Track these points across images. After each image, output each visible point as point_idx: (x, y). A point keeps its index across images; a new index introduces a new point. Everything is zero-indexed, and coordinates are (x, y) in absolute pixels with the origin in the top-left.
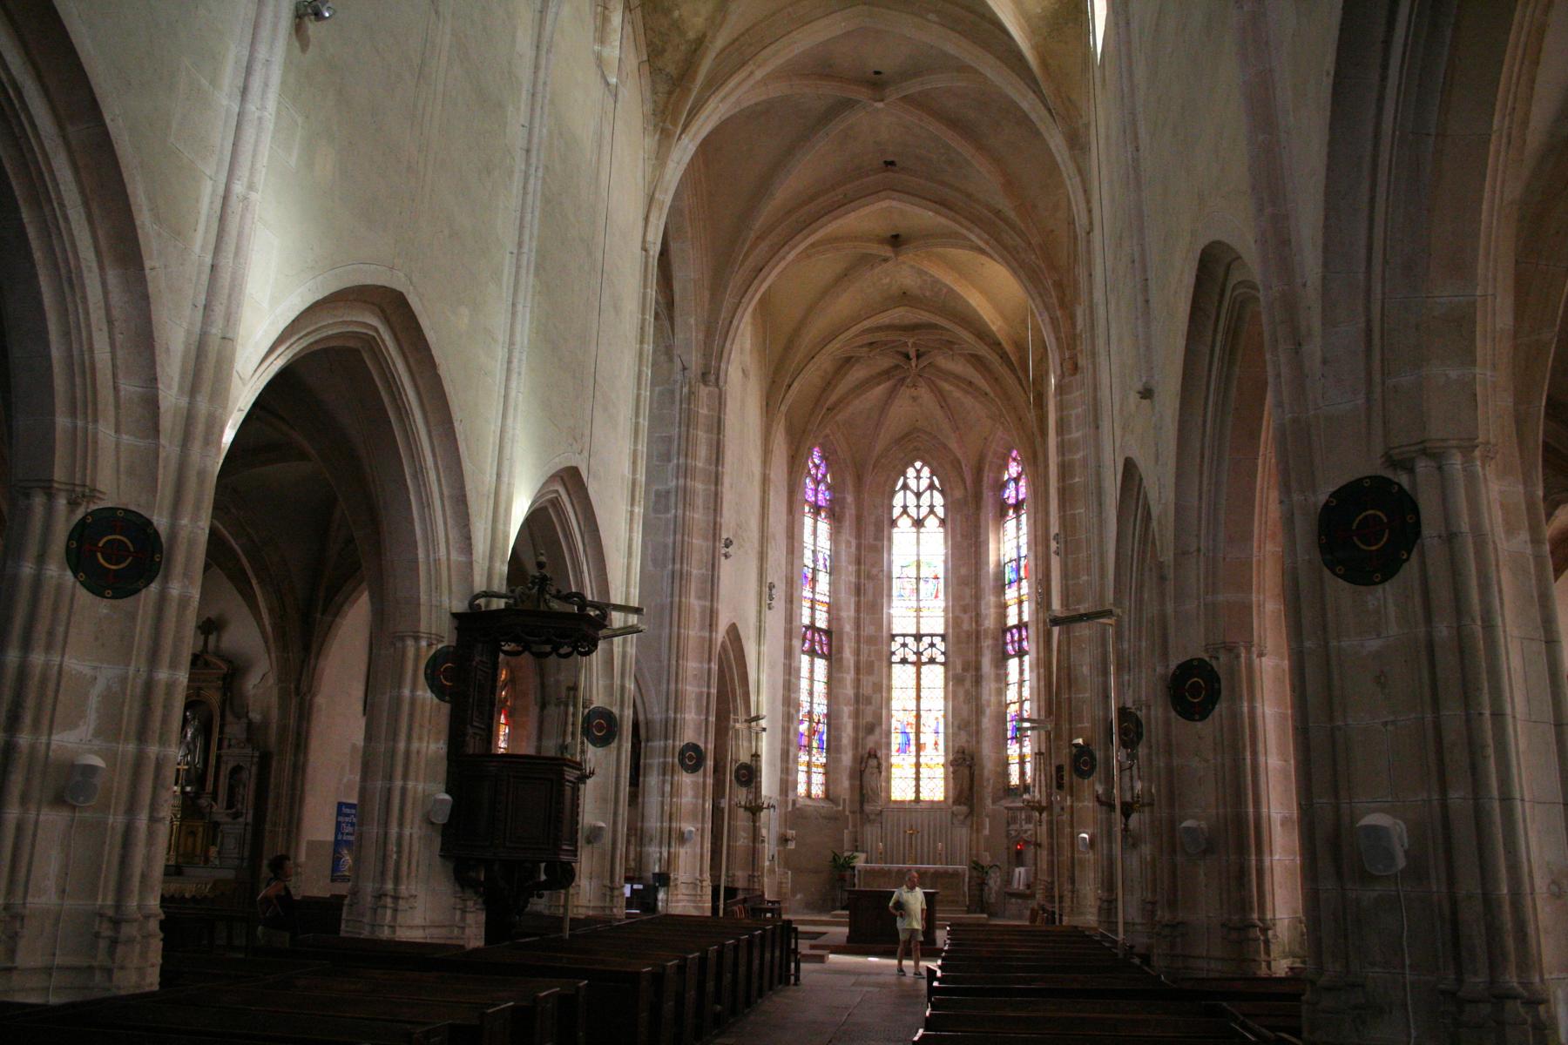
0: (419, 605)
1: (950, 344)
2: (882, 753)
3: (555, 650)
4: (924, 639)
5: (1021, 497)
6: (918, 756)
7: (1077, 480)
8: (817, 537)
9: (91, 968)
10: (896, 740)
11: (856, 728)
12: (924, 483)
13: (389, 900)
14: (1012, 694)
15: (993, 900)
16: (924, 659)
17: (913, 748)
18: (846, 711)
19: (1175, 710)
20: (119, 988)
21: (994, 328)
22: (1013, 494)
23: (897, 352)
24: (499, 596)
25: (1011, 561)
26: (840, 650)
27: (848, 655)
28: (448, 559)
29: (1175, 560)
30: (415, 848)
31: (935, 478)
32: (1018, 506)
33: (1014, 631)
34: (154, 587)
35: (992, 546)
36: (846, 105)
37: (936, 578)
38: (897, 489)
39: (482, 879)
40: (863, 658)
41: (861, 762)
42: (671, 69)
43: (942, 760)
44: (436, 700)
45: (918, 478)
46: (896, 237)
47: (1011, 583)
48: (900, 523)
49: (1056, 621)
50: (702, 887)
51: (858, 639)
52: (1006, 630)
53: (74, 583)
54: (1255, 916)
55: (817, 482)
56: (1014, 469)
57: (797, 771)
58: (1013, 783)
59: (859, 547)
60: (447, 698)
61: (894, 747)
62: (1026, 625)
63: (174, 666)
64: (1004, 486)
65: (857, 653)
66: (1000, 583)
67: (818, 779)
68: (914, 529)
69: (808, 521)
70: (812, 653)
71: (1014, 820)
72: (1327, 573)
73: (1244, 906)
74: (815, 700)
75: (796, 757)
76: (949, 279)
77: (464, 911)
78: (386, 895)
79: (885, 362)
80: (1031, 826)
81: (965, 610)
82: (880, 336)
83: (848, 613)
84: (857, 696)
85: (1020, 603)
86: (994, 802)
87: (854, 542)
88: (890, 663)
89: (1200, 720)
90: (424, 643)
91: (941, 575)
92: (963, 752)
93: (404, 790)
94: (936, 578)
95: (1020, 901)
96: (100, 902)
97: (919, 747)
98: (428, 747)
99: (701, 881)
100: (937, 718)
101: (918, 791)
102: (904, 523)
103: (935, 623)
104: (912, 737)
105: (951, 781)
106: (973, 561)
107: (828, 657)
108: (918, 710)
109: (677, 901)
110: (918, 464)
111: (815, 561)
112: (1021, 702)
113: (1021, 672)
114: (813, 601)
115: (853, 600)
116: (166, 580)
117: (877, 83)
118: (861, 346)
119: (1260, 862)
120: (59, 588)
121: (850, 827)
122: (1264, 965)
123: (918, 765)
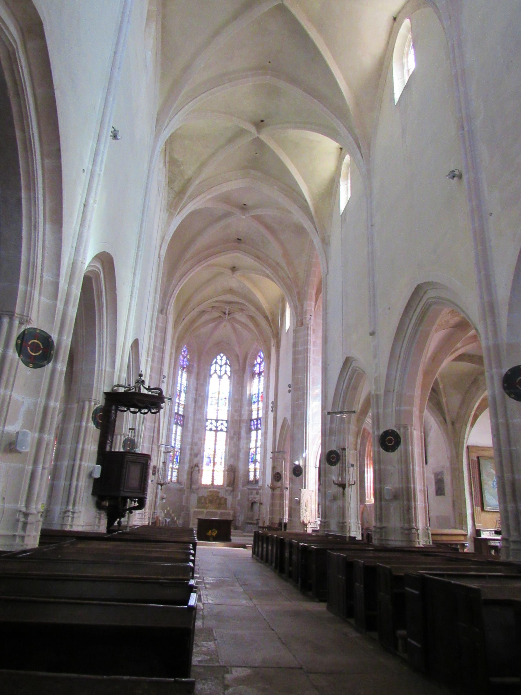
0: (93, 387)
1: (242, 310)
2: (200, 465)
3: (140, 411)
4: (219, 421)
5: (261, 370)
6: (214, 467)
7: (300, 365)
8: (183, 378)
9: (14, 536)
10: (205, 460)
11: (191, 455)
12: (224, 362)
13: (70, 513)
14: (252, 445)
15: (240, 525)
16: (219, 429)
17: (212, 464)
18: (188, 447)
19: (382, 448)
20: (27, 545)
21: (264, 306)
22: (258, 369)
23: (222, 311)
24: (122, 386)
25: (255, 394)
26: (187, 423)
27: (190, 426)
28: (105, 370)
29: (385, 393)
30: (82, 491)
31: (228, 360)
32: (260, 374)
33: (255, 421)
34: (50, 365)
35: (248, 388)
36: (227, 215)
37: (225, 399)
38: (213, 363)
39: (107, 505)
40: (196, 427)
41: (192, 468)
42: (177, 189)
43: (223, 469)
44: (95, 428)
45: (221, 360)
46: (234, 267)
47: (255, 402)
48: (213, 376)
49: (329, 413)
50: (145, 515)
51: (194, 421)
52: (251, 420)
53: (19, 359)
54: (414, 524)
55: (184, 357)
56: (259, 360)
57: (168, 471)
58: (250, 479)
59: (197, 384)
60: (99, 428)
61: (205, 463)
62: (260, 419)
63: (56, 401)
64: (254, 366)
65: (193, 425)
66: (250, 402)
67: (175, 474)
68: (218, 379)
69: (180, 372)
70: (177, 424)
71: (251, 494)
72: (507, 396)
73: (409, 521)
74: (177, 443)
75: (169, 465)
76: (249, 285)
77: (100, 519)
78: (69, 511)
79: (216, 314)
80: (258, 496)
81: (236, 411)
82: (216, 305)
83: (191, 409)
84: (192, 441)
85: (258, 410)
86: (243, 487)
87: (195, 382)
88: (206, 430)
89: (391, 452)
90: (93, 403)
91: (227, 398)
92: (232, 466)
93: (80, 466)
94: (225, 399)
95: (252, 526)
96: (19, 505)
97: (214, 464)
98: (91, 447)
99: (145, 513)
101: (213, 481)
102: (215, 377)
103: (224, 415)
104: (212, 459)
105: (226, 477)
107: (182, 426)
108: (215, 449)
109: (135, 521)
110: (222, 355)
111: (181, 388)
112: (256, 448)
113: (257, 436)
114: (179, 404)
115: (193, 404)
116: (56, 361)
117: (244, 208)
118: (210, 307)
119: (415, 504)
120: (12, 360)
121: (186, 494)
122: (417, 543)
123: (213, 471)
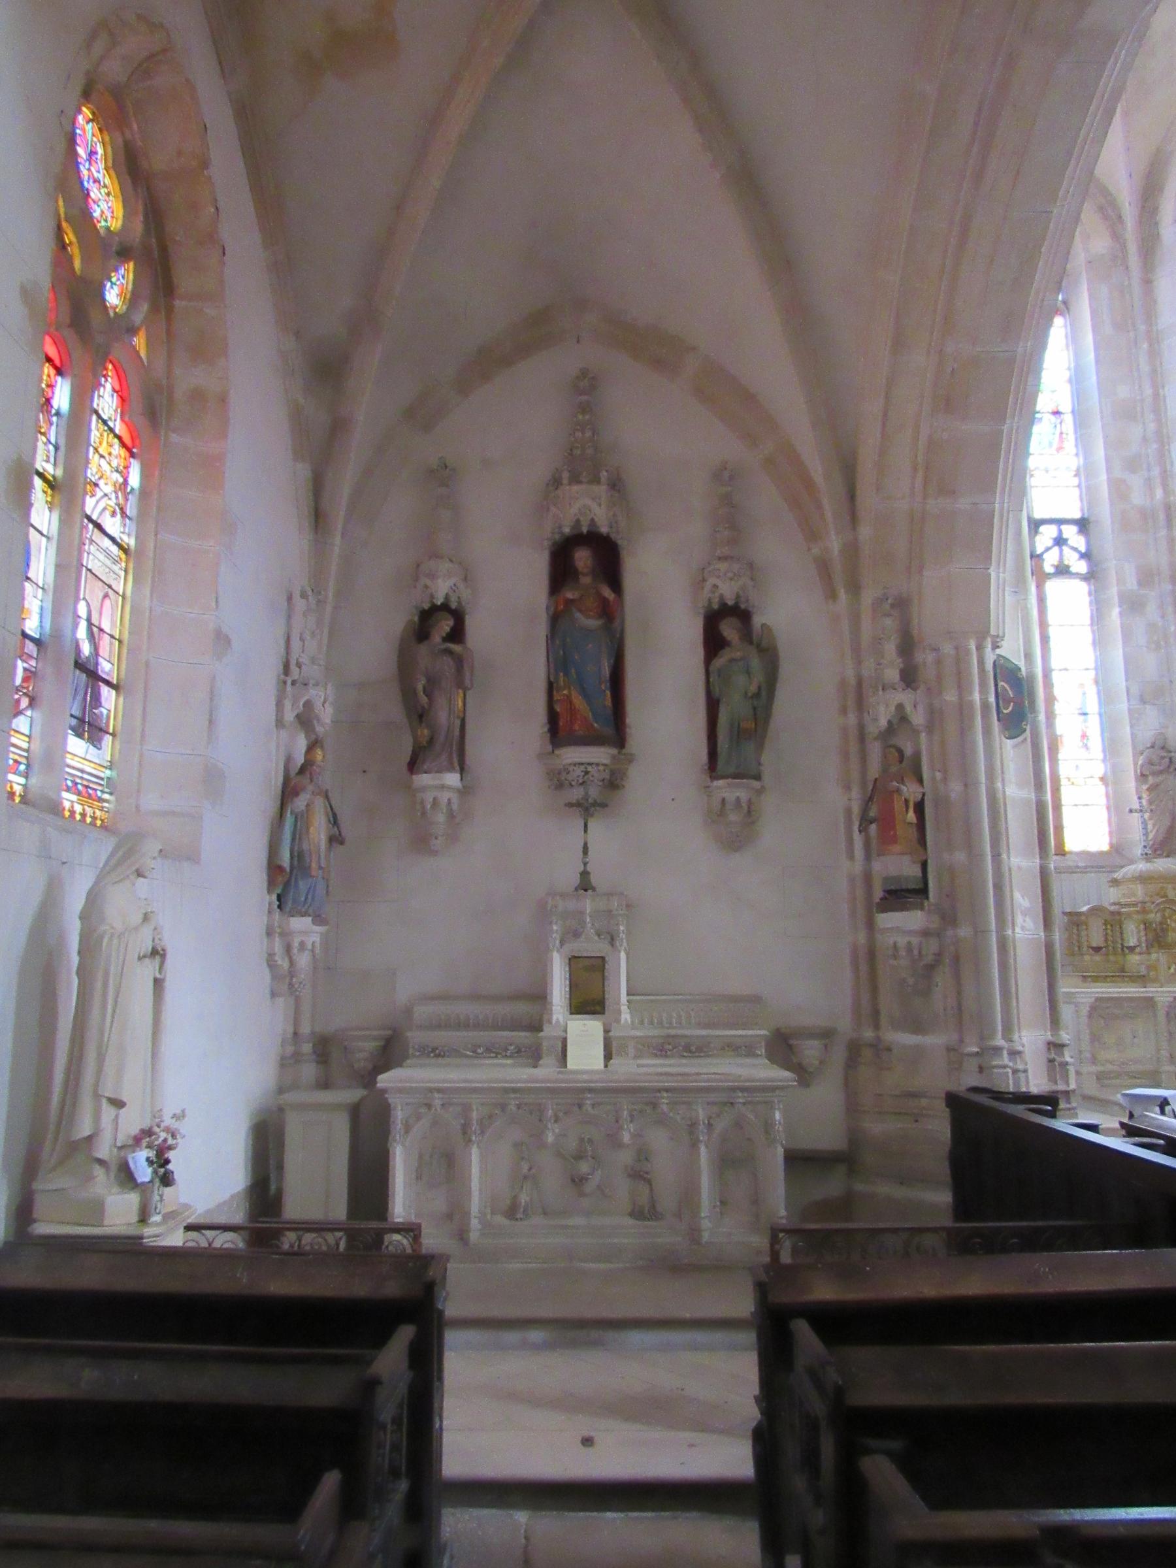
4: (1042, 529)
16: (1048, 568)
37: (1056, 413)
81: (1132, 465)
100: (1082, 685)
106: (1145, 367)
